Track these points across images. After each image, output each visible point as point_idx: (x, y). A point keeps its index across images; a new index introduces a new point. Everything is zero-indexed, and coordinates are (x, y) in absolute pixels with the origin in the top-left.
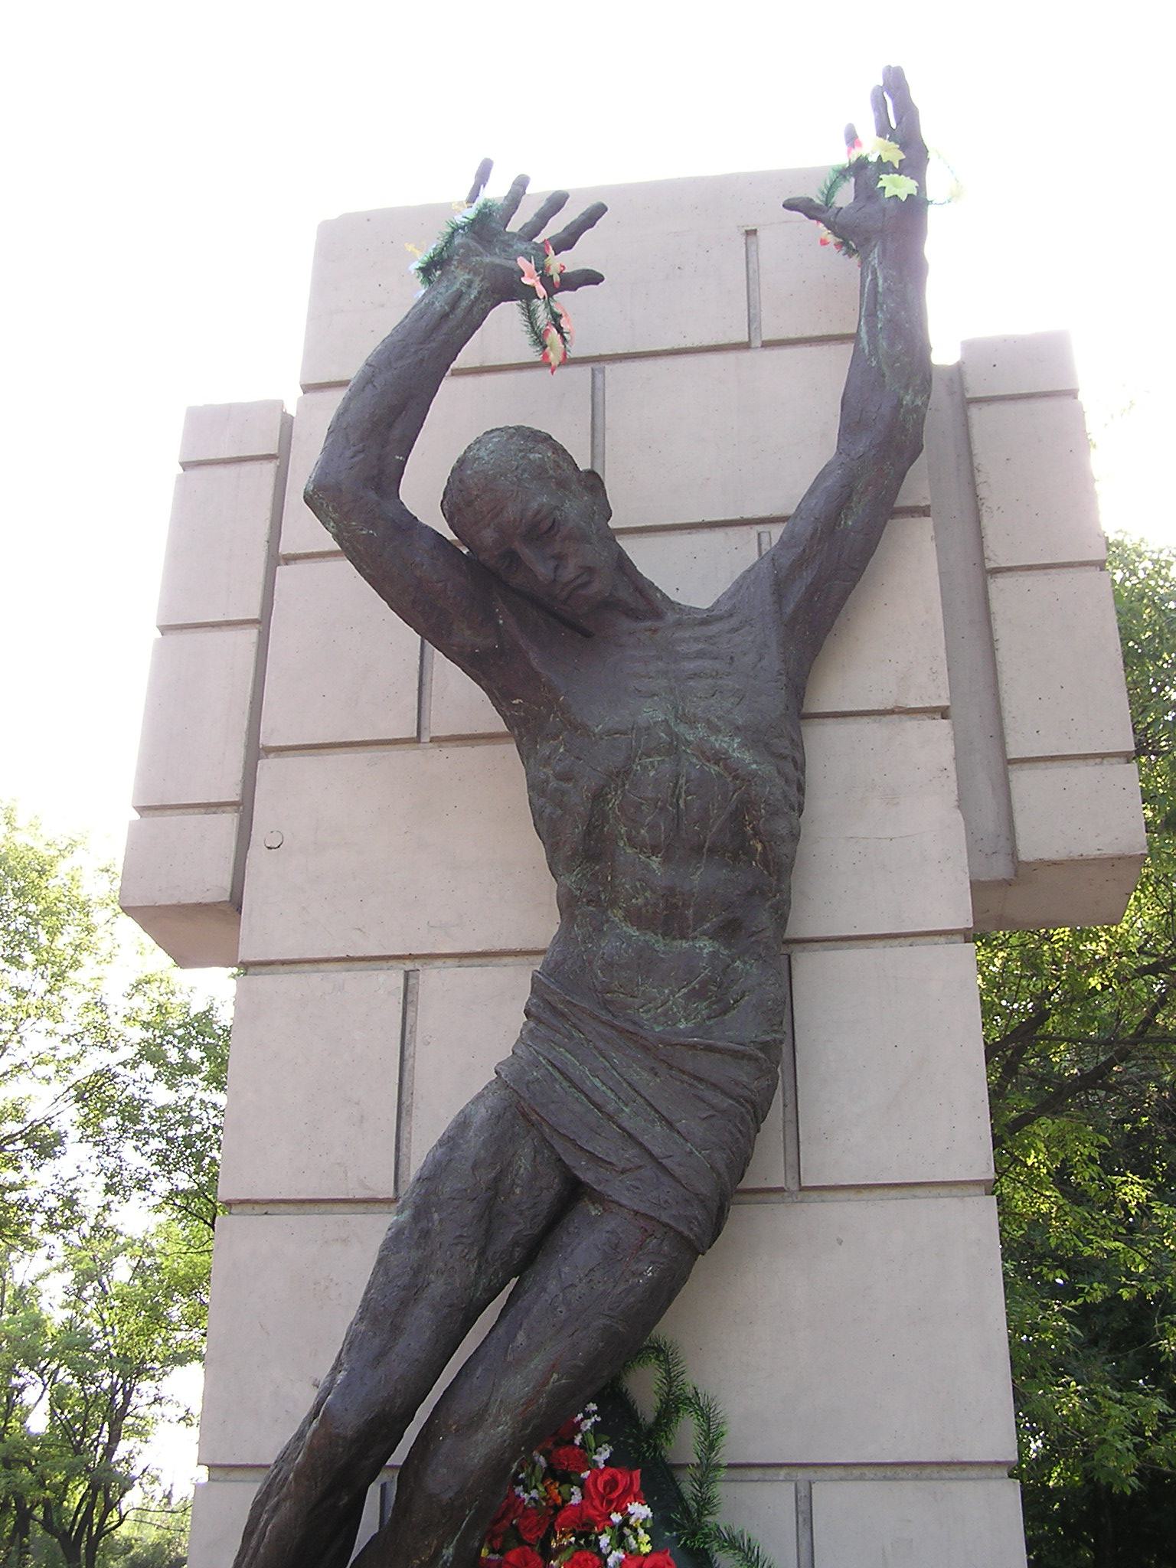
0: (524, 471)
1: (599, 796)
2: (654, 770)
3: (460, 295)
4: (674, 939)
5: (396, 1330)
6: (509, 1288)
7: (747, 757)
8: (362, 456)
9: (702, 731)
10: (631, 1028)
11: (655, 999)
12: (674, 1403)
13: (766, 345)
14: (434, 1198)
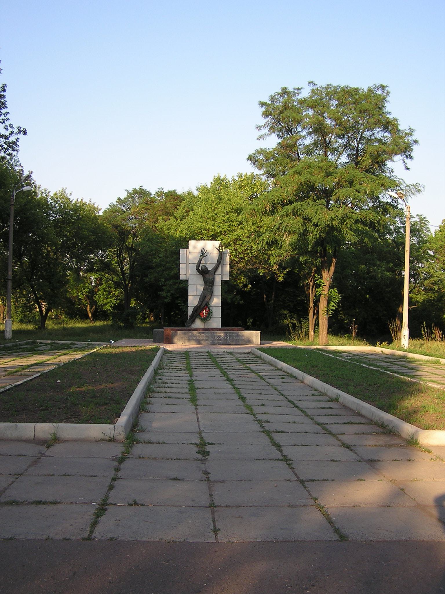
12: (209, 304)
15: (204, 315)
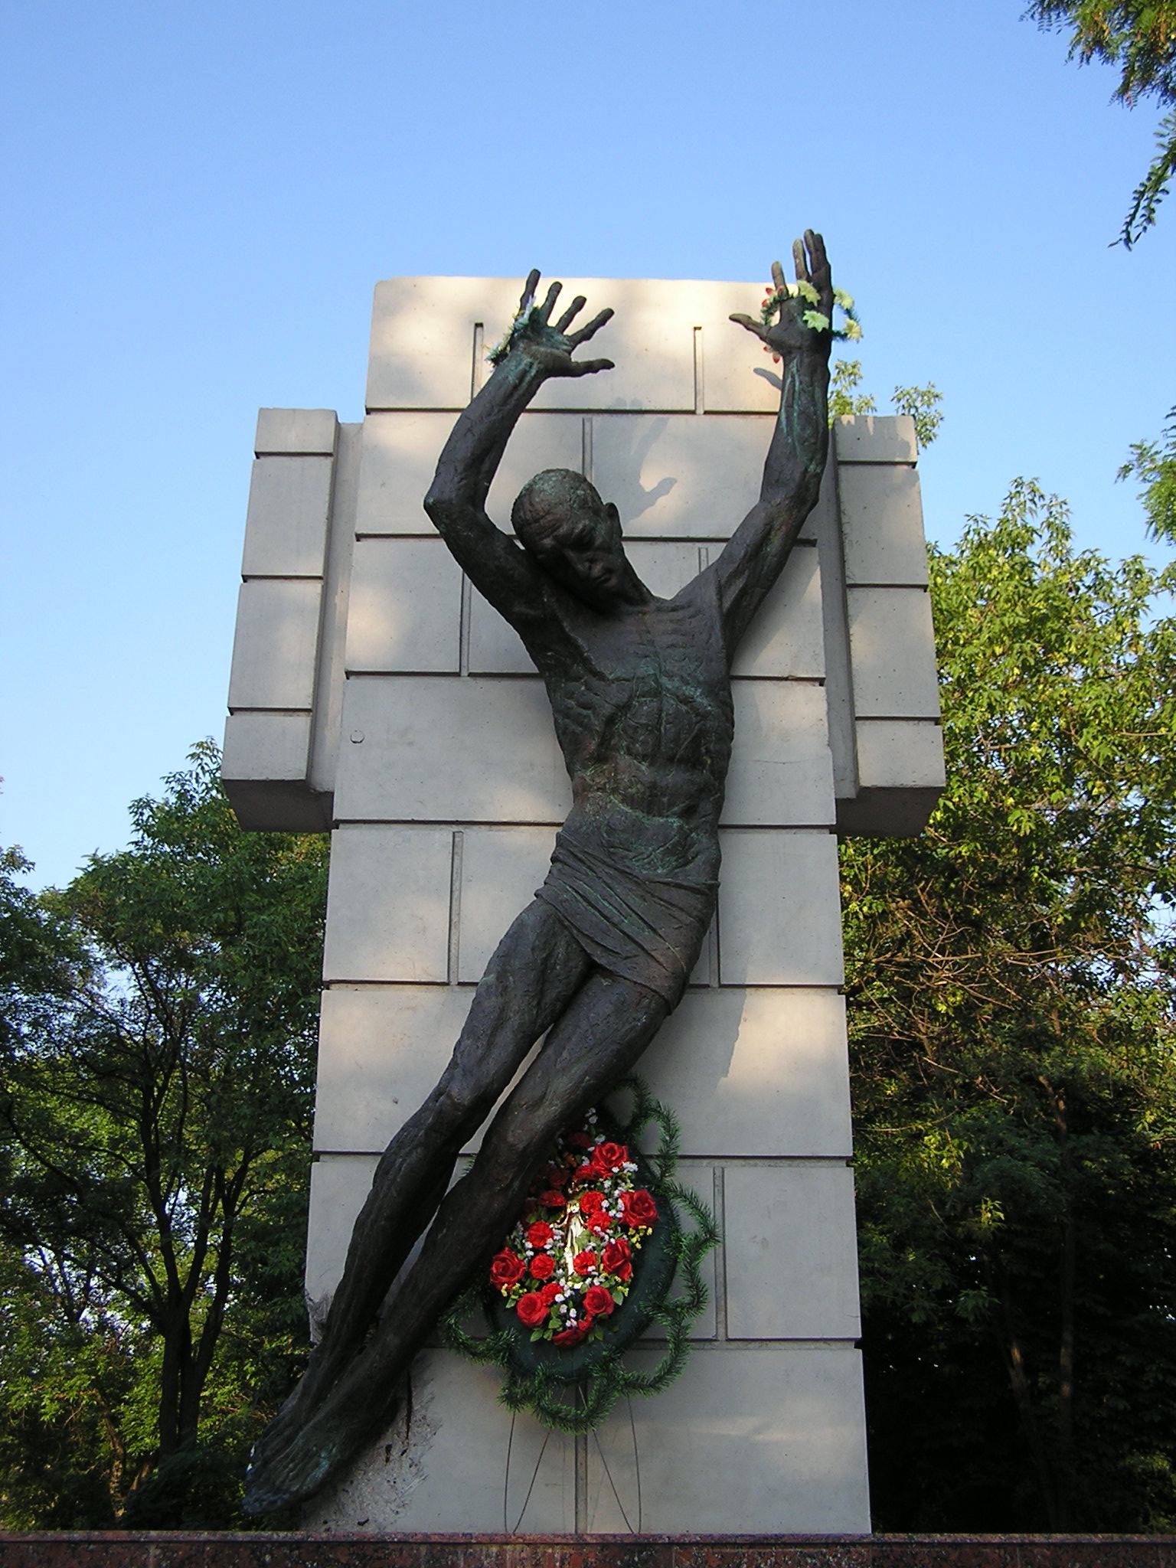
0: (574, 502)
1: (610, 721)
2: (645, 708)
3: (525, 373)
4: (654, 816)
5: (490, 1045)
6: (550, 1028)
7: (705, 702)
8: (464, 482)
9: (677, 684)
10: (628, 870)
11: (642, 853)
12: (645, 1111)
13: (706, 413)
14: (508, 968)
15: (569, 1286)
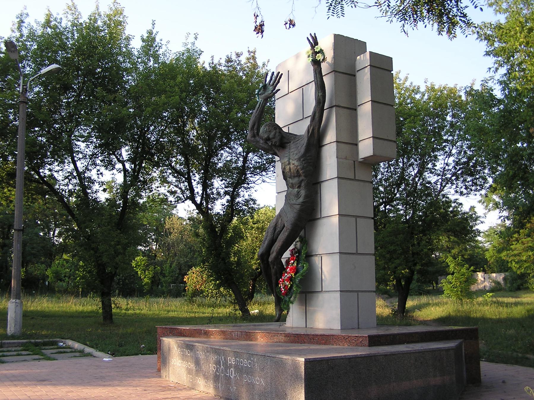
3: (260, 103)
